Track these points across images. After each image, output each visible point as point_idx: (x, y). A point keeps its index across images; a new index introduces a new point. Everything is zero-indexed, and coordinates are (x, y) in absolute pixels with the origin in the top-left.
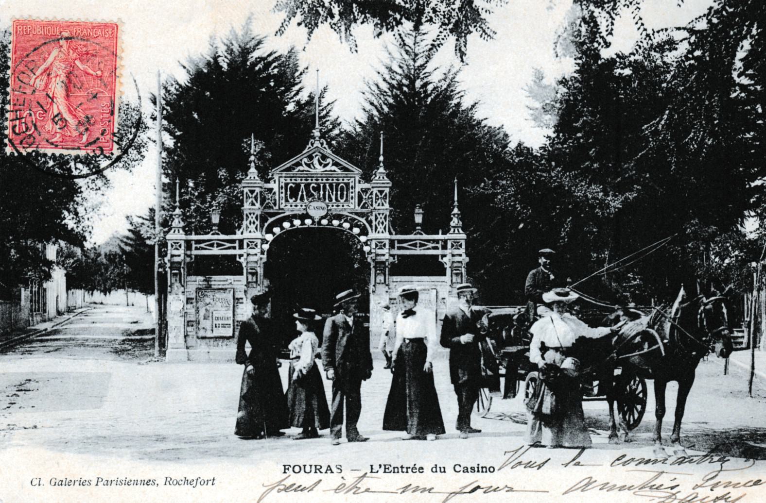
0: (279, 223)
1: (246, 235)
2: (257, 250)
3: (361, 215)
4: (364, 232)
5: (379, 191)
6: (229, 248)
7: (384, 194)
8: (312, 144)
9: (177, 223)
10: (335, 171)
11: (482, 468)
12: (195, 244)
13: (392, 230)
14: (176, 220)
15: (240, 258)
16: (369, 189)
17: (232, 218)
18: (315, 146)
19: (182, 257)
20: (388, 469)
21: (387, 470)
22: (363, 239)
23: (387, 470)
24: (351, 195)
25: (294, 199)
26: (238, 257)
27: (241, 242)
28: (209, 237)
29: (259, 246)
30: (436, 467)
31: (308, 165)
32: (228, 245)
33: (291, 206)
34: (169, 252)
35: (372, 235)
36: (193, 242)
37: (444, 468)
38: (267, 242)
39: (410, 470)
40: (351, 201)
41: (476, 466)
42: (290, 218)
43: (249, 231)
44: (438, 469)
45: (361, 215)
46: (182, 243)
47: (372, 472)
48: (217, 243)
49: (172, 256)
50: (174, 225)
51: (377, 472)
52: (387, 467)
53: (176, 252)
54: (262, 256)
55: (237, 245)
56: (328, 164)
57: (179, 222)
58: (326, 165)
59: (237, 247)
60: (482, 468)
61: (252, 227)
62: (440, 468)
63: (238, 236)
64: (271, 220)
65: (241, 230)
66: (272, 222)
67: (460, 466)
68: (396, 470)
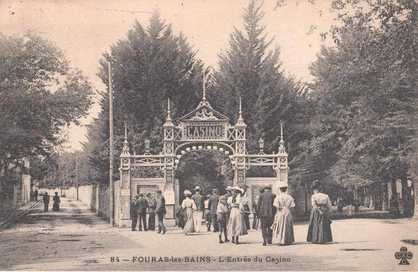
0: (184, 148)
1: (166, 155)
2: (172, 164)
3: (229, 143)
4: (231, 153)
5: (239, 130)
6: (156, 162)
7: (242, 132)
8: (202, 104)
9: (125, 148)
10: (214, 119)
11: (283, 259)
12: (250, 159)
13: (247, 152)
14: (125, 147)
15: (162, 168)
16: (234, 129)
17: (156, 146)
18: (203, 105)
19: (129, 168)
20: (230, 259)
21: (229, 260)
22: (231, 157)
23: (229, 260)
24: (223, 132)
25: (192, 135)
26: (160, 167)
27: (163, 158)
28: (144, 156)
29: (173, 161)
30: (257, 259)
31: (200, 116)
32: (155, 160)
33: (190, 139)
34: (121, 164)
35: (236, 154)
36: (249, 159)
37: (261, 259)
38: (177, 159)
39: (243, 260)
40: (223, 136)
41: (279, 258)
42: (190, 146)
43: (168, 152)
44: (258, 260)
45: (229, 143)
46: (129, 160)
47: (220, 261)
48: (149, 160)
49: (123, 167)
50: (124, 149)
51: (223, 261)
52: (229, 258)
53: (125, 165)
54: (174, 167)
55: (273, 160)
56: (210, 115)
57: (127, 148)
58: (209, 116)
59: (274, 161)
60: (283, 259)
61: (169, 150)
62: (259, 259)
63: (161, 155)
64: (179, 146)
65: (163, 152)
66: (180, 148)
67: (270, 257)
68: (234, 260)
